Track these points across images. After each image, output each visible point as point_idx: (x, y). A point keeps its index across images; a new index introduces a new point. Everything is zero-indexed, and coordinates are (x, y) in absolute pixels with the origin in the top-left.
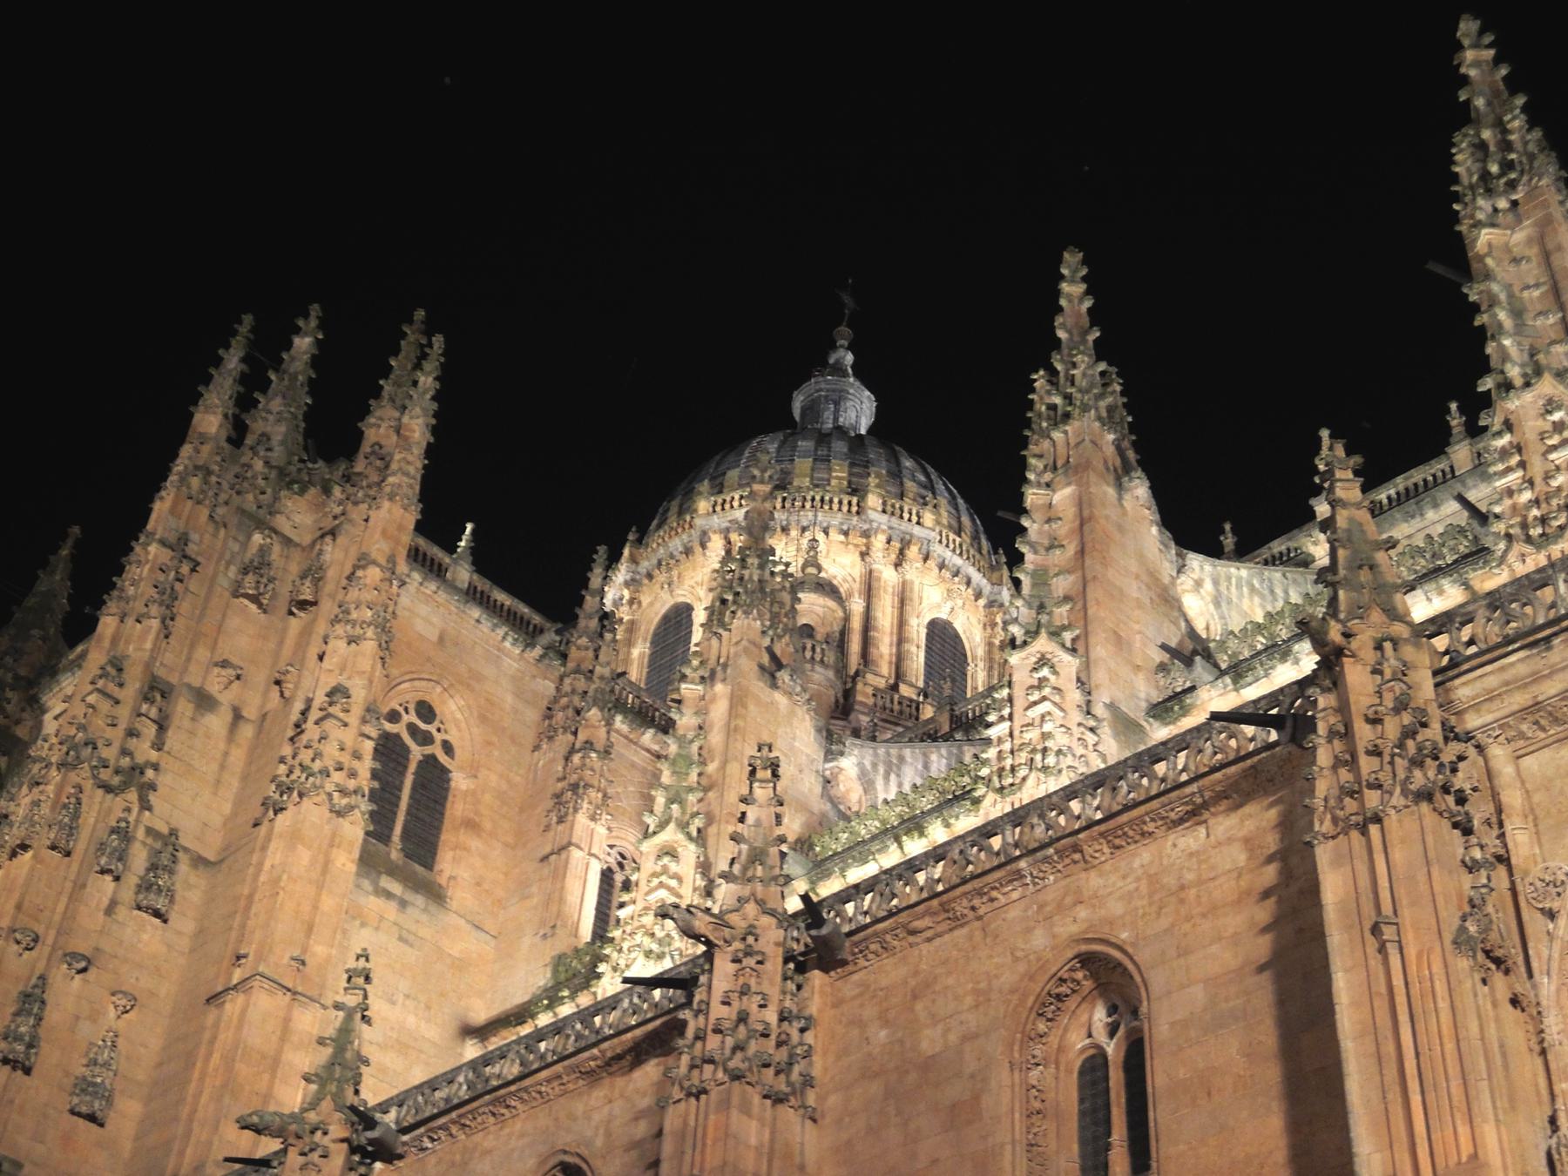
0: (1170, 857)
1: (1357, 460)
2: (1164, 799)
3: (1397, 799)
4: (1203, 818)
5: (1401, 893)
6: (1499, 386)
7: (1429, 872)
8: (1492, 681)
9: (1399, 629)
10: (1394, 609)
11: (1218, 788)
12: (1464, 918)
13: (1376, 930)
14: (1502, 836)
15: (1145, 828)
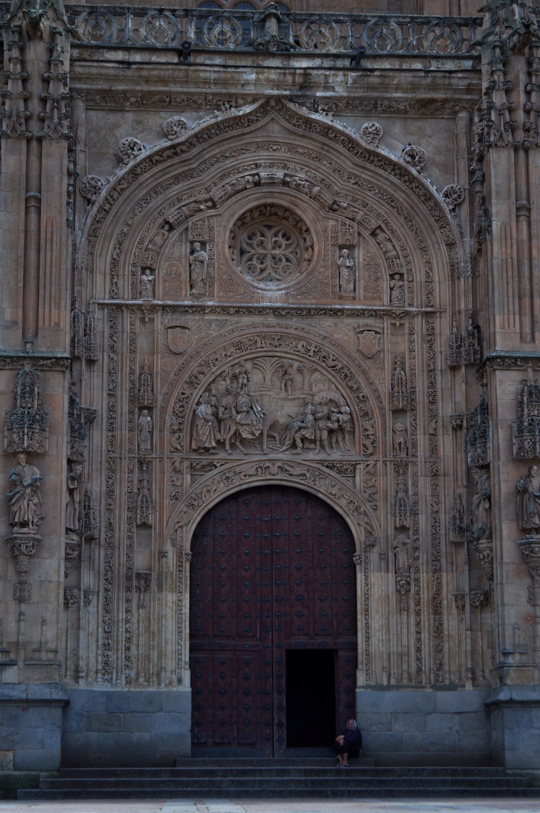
8: (94, 71)
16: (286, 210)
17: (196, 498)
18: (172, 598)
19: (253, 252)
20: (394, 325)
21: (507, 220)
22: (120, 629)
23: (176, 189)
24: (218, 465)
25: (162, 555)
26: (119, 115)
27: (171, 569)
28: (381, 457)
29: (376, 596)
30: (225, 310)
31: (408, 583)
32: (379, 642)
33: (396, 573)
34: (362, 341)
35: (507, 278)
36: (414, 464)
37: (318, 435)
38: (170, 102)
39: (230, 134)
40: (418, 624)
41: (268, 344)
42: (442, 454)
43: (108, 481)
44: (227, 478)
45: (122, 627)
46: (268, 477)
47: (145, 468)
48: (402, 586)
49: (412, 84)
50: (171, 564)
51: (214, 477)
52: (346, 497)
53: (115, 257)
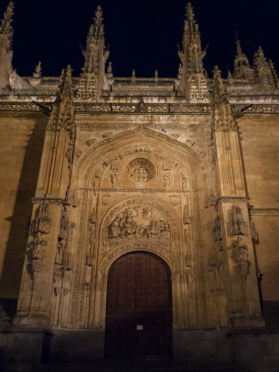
0: (11, 122)
1: (72, 70)
2: (14, 112)
3: (63, 129)
4: (20, 118)
5: (59, 144)
6: (86, 70)
7: (65, 143)
8: (82, 117)
9: (71, 101)
10: (71, 98)
11: (26, 114)
12: (67, 152)
13: (53, 148)
14: (74, 142)
15: (8, 116)
16: (146, 160)
19: (135, 175)
20: (184, 195)
21: (223, 154)
23: (108, 153)
26: (91, 132)
30: (124, 190)
34: (172, 201)
35: (224, 172)
37: (157, 233)
38: (108, 127)
39: (127, 136)
41: (139, 202)
49: (187, 119)
53: (86, 174)
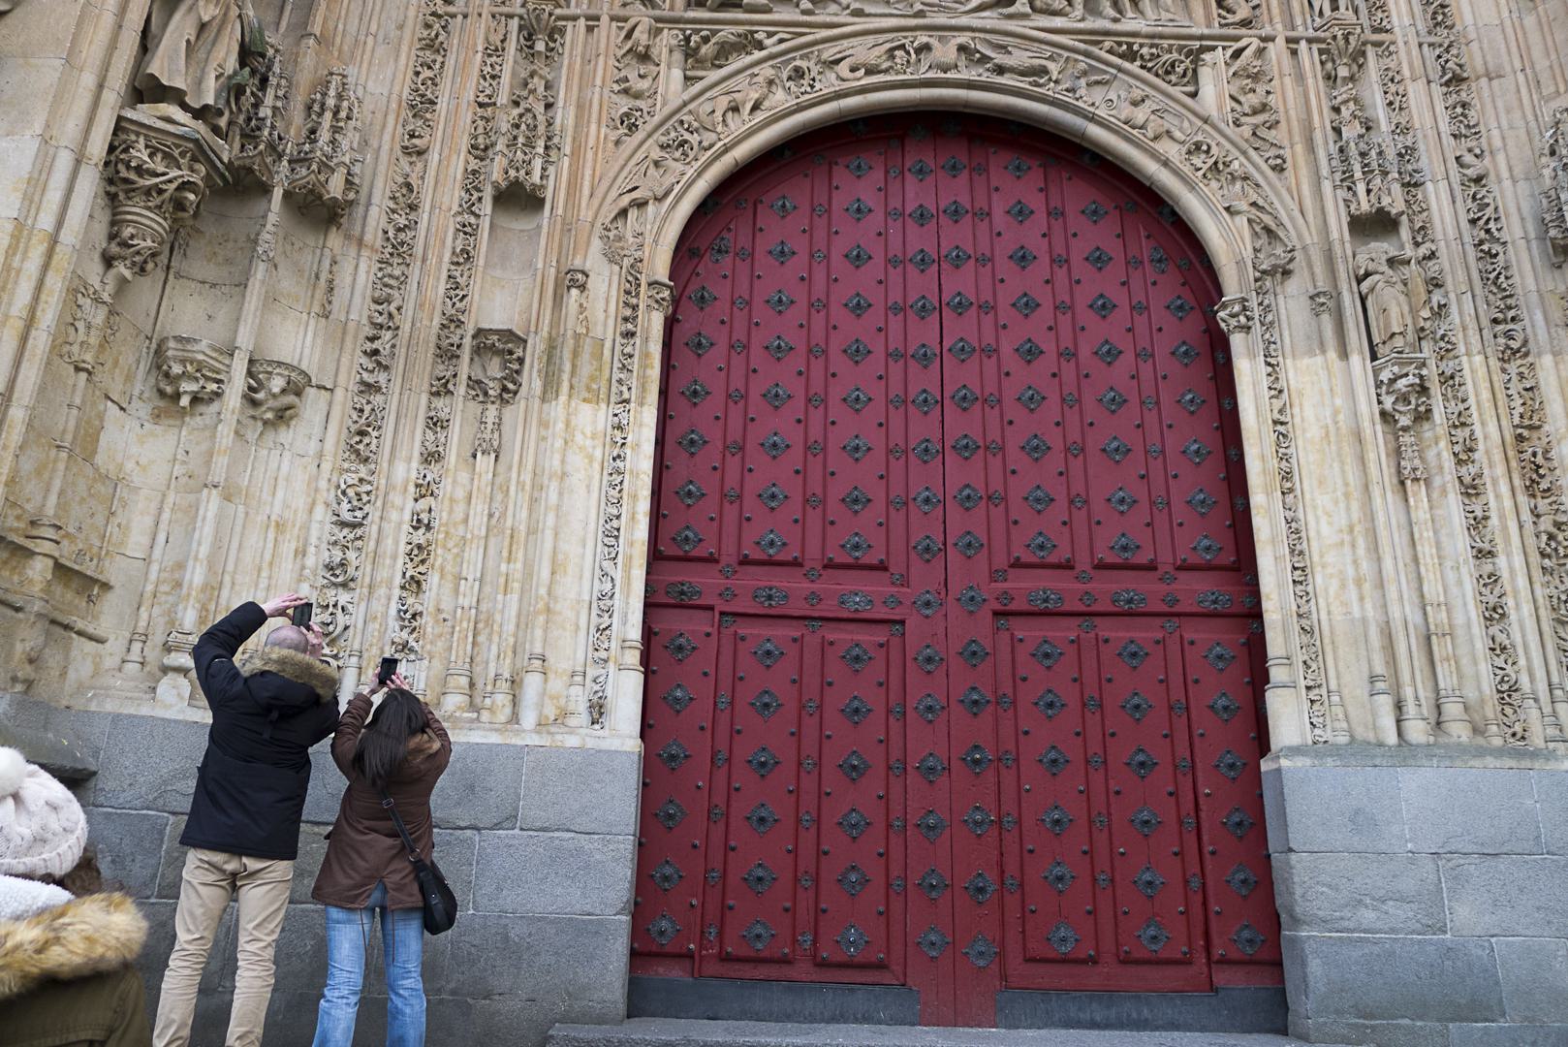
17: (696, 124)
18: (594, 422)
22: (394, 516)
24: (768, 42)
25: (574, 280)
27: (598, 332)
28: (1279, 27)
29: (1314, 432)
31: (1423, 390)
32: (1343, 586)
33: (1374, 357)
36: (1385, 49)
40: (1477, 523)
42: (1469, 19)
43: (417, 74)
44: (798, 74)
45: (402, 508)
46: (930, 75)
47: (540, 46)
48: (1404, 398)
50: (601, 316)
51: (756, 70)
52: (1178, 134)
